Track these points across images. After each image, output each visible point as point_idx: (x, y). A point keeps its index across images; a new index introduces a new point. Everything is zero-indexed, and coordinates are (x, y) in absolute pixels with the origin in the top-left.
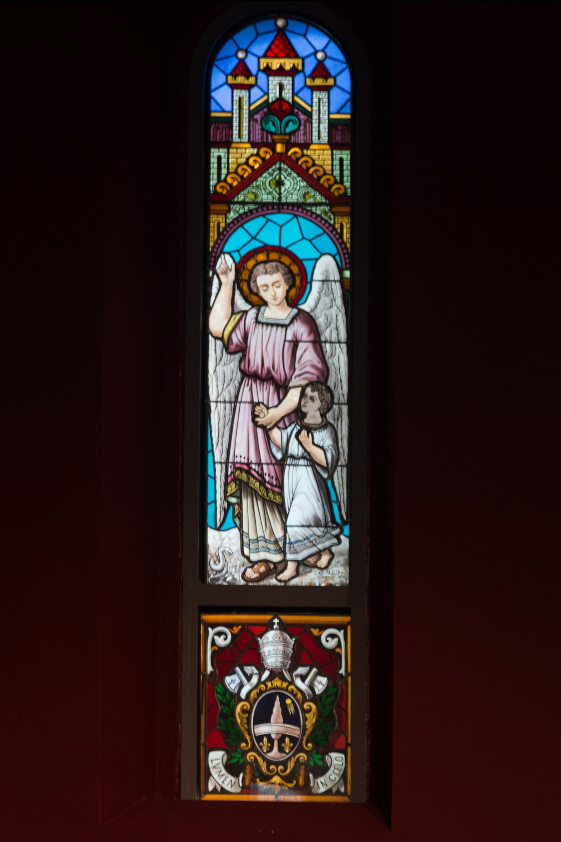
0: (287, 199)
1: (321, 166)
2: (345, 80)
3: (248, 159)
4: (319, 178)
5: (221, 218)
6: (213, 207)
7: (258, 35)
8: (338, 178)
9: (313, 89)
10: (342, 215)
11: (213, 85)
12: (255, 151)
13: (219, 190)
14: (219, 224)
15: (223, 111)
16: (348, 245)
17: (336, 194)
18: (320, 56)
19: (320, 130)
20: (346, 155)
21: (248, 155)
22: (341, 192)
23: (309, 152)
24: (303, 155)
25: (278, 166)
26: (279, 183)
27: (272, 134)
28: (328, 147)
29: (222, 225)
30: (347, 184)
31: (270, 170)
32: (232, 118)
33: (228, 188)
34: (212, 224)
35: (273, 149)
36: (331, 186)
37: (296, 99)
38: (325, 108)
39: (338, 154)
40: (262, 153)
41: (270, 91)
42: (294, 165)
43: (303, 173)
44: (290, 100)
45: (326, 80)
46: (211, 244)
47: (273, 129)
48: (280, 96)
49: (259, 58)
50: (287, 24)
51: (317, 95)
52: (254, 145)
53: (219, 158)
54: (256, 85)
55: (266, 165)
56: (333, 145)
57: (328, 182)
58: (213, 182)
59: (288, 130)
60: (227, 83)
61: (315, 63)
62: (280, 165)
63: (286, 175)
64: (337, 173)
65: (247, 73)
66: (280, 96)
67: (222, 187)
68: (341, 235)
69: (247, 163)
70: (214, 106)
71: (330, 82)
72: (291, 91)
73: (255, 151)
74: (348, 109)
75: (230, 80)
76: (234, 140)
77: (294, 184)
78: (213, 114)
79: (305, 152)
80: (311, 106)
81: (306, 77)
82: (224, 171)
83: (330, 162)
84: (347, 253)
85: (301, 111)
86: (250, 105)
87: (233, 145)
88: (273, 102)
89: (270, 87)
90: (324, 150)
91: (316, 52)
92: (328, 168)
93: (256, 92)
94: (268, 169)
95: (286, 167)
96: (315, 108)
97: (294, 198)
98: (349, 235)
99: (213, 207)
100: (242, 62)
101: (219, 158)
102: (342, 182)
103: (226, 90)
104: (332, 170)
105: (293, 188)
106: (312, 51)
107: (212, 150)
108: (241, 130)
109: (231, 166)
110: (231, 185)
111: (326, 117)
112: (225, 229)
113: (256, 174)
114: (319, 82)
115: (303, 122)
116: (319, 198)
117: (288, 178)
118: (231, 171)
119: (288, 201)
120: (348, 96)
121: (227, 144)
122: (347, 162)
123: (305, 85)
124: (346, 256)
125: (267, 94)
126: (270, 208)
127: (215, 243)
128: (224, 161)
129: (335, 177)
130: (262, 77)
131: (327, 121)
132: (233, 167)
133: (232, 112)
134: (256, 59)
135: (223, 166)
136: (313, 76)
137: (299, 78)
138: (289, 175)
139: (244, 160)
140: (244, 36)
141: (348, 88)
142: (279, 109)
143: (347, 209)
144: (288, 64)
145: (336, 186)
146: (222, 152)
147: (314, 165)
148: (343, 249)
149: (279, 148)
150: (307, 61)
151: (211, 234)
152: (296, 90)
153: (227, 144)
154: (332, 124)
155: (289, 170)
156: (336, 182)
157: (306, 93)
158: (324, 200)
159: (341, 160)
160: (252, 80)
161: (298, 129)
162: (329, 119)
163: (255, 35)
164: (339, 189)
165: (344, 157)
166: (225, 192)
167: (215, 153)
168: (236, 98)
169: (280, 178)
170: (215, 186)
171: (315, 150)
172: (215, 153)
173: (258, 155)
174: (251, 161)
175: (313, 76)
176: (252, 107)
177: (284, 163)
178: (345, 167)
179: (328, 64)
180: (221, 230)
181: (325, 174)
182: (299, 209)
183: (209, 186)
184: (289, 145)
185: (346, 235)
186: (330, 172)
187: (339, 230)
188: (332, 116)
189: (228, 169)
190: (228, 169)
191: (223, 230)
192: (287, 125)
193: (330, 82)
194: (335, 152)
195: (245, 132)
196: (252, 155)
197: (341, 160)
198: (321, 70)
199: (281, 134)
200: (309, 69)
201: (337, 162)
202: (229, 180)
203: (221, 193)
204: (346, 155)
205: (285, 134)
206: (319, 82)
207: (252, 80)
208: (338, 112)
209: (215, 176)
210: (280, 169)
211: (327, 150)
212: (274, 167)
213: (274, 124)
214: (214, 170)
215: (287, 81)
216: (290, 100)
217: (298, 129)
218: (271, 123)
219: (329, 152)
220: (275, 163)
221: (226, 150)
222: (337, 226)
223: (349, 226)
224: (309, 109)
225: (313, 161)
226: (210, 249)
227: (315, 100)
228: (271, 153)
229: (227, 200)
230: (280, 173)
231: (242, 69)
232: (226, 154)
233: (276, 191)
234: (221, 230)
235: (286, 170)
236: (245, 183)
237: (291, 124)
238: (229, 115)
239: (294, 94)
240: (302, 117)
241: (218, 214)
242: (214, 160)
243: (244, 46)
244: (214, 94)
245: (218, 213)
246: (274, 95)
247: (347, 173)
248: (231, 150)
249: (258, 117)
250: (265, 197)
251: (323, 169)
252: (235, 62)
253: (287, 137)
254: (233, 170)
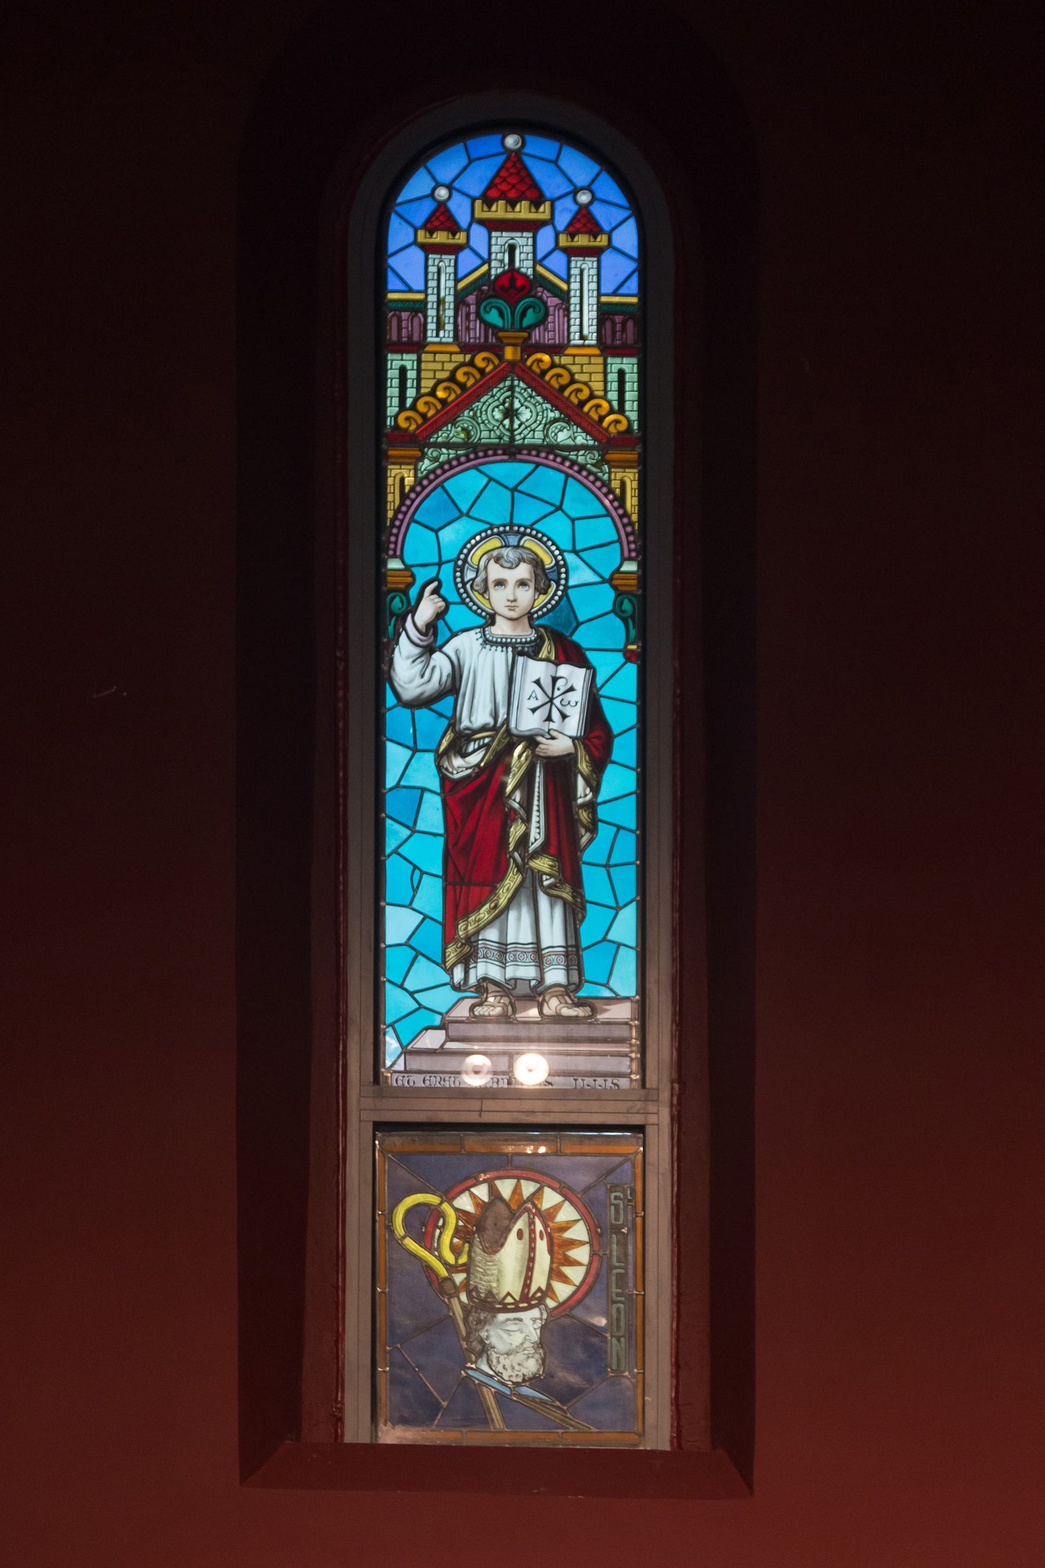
1: (585, 384)
2: (627, 237)
3: (453, 372)
8: (615, 404)
9: (571, 252)
10: (624, 465)
12: (468, 357)
13: (403, 424)
14: (402, 480)
15: (411, 290)
16: (635, 518)
19: (585, 321)
20: (629, 365)
21: (450, 366)
22: (623, 427)
24: (553, 365)
25: (508, 383)
28: (597, 351)
29: (409, 481)
30: (633, 416)
32: (425, 302)
33: (420, 421)
34: (390, 481)
35: (500, 357)
37: (539, 268)
38: (593, 286)
39: (615, 364)
40: (479, 361)
42: (537, 383)
43: (555, 397)
46: (390, 514)
48: (514, 261)
51: (577, 262)
52: (465, 348)
53: (403, 371)
55: (486, 384)
58: (392, 410)
59: (526, 322)
60: (415, 242)
64: (613, 396)
65: (453, 227)
66: (514, 261)
67: (407, 419)
68: (621, 500)
69: (452, 378)
70: (393, 283)
71: (602, 241)
72: (530, 256)
74: (633, 285)
78: (391, 296)
79: (556, 359)
80: (568, 282)
82: (411, 393)
83: (601, 377)
86: (457, 281)
89: (494, 249)
92: (597, 386)
98: (635, 501)
101: (403, 371)
102: (621, 410)
103: (418, 254)
104: (605, 391)
107: (390, 356)
109: (423, 383)
110: (424, 416)
112: (412, 489)
113: (469, 397)
114: (582, 240)
121: (417, 346)
126: (490, 452)
127: (397, 511)
128: (411, 374)
129: (610, 402)
130: (478, 233)
133: (425, 291)
134: (467, 203)
135: (409, 383)
137: (546, 236)
140: (448, 164)
142: (512, 287)
144: (523, 211)
145: (612, 417)
146: (409, 360)
147: (573, 381)
149: (509, 353)
150: (559, 205)
151: (390, 498)
152: (539, 256)
154: (605, 313)
155: (529, 390)
156: (611, 411)
157: (558, 261)
158: (591, 443)
159: (621, 373)
164: (617, 422)
165: (627, 368)
166: (413, 427)
168: (432, 269)
170: (396, 417)
172: (395, 362)
174: (460, 376)
175: (572, 230)
176: (461, 285)
180: (407, 489)
184: (529, 348)
185: (631, 502)
186: (602, 393)
187: (618, 491)
188: (604, 299)
189: (418, 388)
190: (418, 388)
192: (523, 315)
193: (602, 241)
197: (621, 373)
198: (584, 221)
200: (562, 220)
201: (613, 377)
202: (421, 406)
204: (629, 365)
205: (521, 329)
206: (582, 240)
208: (614, 294)
209: (396, 401)
213: (501, 315)
215: (522, 240)
216: (530, 272)
219: (600, 360)
221: (414, 357)
222: (615, 484)
223: (635, 484)
224: (564, 286)
225: (572, 375)
227: (575, 271)
229: (417, 441)
230: (512, 396)
231: (441, 218)
236: (449, 413)
237: (530, 312)
238: (421, 296)
239: (536, 262)
240: (552, 301)
242: (393, 374)
244: (392, 261)
245: (400, 462)
247: (631, 395)
248: (424, 357)
251: (590, 388)
253: (525, 335)
254: (427, 390)
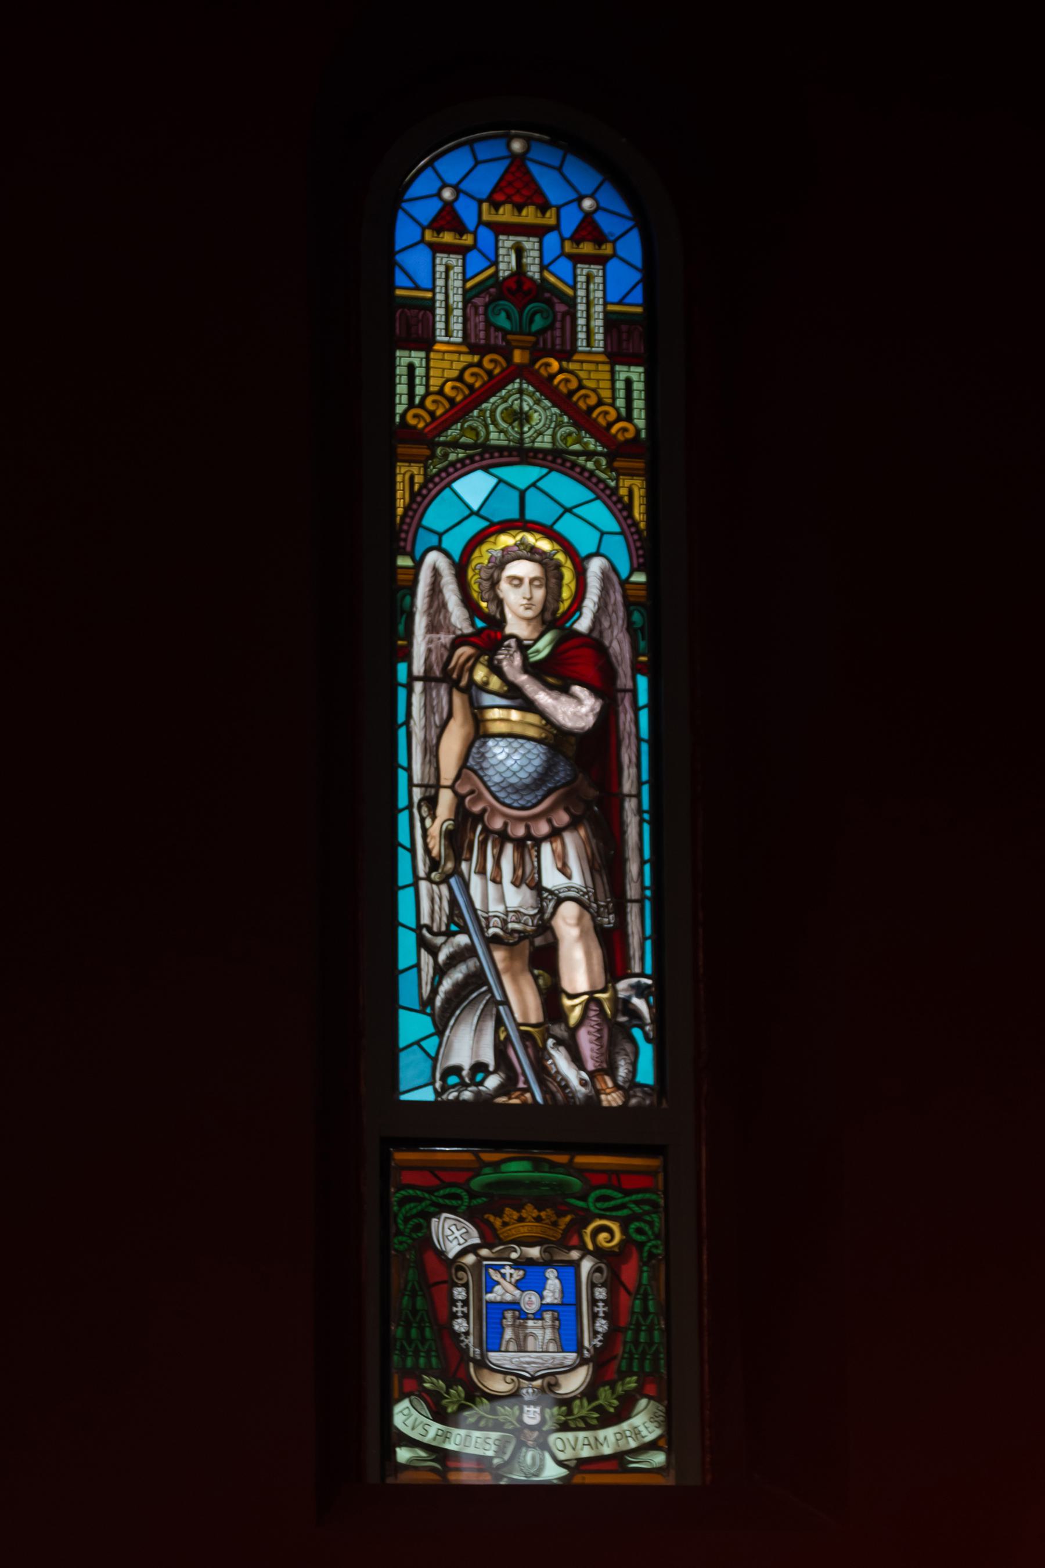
0: (533, 442)
1: (594, 390)
2: (632, 247)
3: (462, 371)
4: (591, 409)
5: (415, 469)
6: (401, 450)
7: (477, 163)
8: (623, 411)
10: (632, 474)
11: (400, 243)
12: (476, 358)
13: (411, 421)
14: (412, 478)
15: (417, 288)
16: (642, 525)
17: (620, 437)
18: (587, 204)
19: (591, 329)
20: (636, 374)
21: (460, 366)
22: (630, 435)
23: (572, 366)
25: (516, 386)
26: (521, 417)
27: (505, 332)
28: (602, 358)
29: (419, 479)
30: (641, 423)
31: (504, 392)
32: (433, 300)
33: (428, 419)
34: (399, 478)
35: (508, 358)
36: (610, 425)
37: (547, 275)
38: (601, 291)
39: (623, 372)
40: (487, 364)
41: (501, 259)
42: (545, 387)
43: (563, 401)
44: (537, 276)
45: (600, 246)
46: (400, 511)
47: (507, 325)
49: (480, 202)
50: (528, 150)
51: (583, 270)
53: (411, 368)
54: (474, 246)
55: (494, 385)
56: (616, 355)
57: (605, 417)
58: (400, 409)
59: (535, 328)
60: (422, 240)
61: (580, 216)
62: (521, 384)
63: (531, 403)
64: (620, 403)
65: (460, 229)
67: (415, 416)
68: (629, 507)
69: (460, 378)
70: (400, 279)
73: (476, 358)
74: (638, 296)
75: (429, 236)
76: (438, 338)
77: (546, 418)
78: (399, 292)
79: (564, 364)
80: (574, 288)
81: (563, 240)
82: (420, 390)
84: (640, 540)
85: (557, 297)
86: (465, 280)
87: (437, 347)
88: (505, 279)
89: (502, 251)
90: (597, 363)
91: (580, 199)
92: (606, 394)
93: (475, 260)
94: (500, 390)
95: (531, 389)
96: (581, 293)
97: (545, 442)
98: (643, 508)
99: (401, 450)
100: (448, 208)
101: (411, 368)
102: (629, 418)
103: (422, 254)
104: (614, 398)
105: (544, 425)
106: (574, 196)
107: (398, 353)
108: (450, 327)
109: (432, 382)
110: (432, 414)
111: (599, 308)
112: (423, 486)
113: (477, 397)
115: (559, 317)
116: (592, 444)
117: (536, 407)
118: (432, 389)
119: (537, 445)
120: (637, 276)
121: (426, 343)
122: (638, 386)
123: (563, 254)
124: (638, 544)
125: (495, 263)
127: (407, 509)
128: (420, 372)
129: (617, 409)
130: (485, 235)
131: (601, 316)
132: (435, 383)
133: (433, 290)
134: (474, 205)
136: (577, 238)
137: (552, 240)
138: (538, 402)
139: (455, 374)
141: (639, 263)
142: (519, 289)
143: (639, 464)
144: (529, 215)
146: (417, 357)
147: (581, 387)
148: (629, 526)
149: (518, 357)
151: (399, 494)
152: (546, 261)
153: (426, 343)
154: (612, 322)
156: (619, 419)
158: (600, 449)
159: (629, 382)
160: (468, 240)
161: (551, 327)
162: (606, 314)
163: (470, 163)
164: (624, 430)
165: (634, 377)
166: (421, 425)
167: (403, 358)
168: (440, 269)
169: (521, 408)
170: (403, 416)
171: (582, 362)
172: (403, 358)
173: (479, 364)
175: (577, 238)
176: (469, 285)
177: (529, 383)
178: (635, 395)
179: (601, 218)
180: (416, 487)
181: (600, 403)
182: (555, 459)
183: (394, 414)
184: (537, 353)
185: (639, 512)
186: (609, 401)
187: (626, 499)
188: (610, 308)
189: (427, 386)
190: (427, 386)
191: (420, 489)
194: (618, 368)
195: (457, 327)
196: (471, 365)
197: (629, 382)
198: (588, 229)
199: (521, 333)
201: (620, 385)
203: (415, 427)
204: (636, 374)
205: (530, 334)
206: (587, 248)
207: (468, 240)
208: (620, 303)
209: (405, 399)
210: (521, 391)
211: (603, 363)
212: (510, 387)
213: (509, 317)
214: (402, 389)
215: (530, 244)
216: (537, 276)
217: (551, 327)
218: (503, 314)
219: (607, 367)
220: (512, 381)
221: (422, 354)
223: (643, 491)
224: (570, 292)
225: (580, 380)
226: (398, 519)
227: (581, 279)
228: (504, 364)
230: (522, 400)
232: (424, 361)
233: (513, 428)
234: (416, 487)
235: (531, 395)
236: (459, 411)
237: (538, 317)
238: (429, 295)
239: (543, 267)
240: (560, 308)
241: (410, 461)
242: (401, 370)
243: (454, 180)
244: (399, 258)
245: (410, 460)
246: (507, 265)
247: (639, 404)
248: (432, 355)
249: (478, 301)
250: (495, 438)
251: (598, 395)
252: (435, 206)
253: (532, 339)
254: (436, 389)
